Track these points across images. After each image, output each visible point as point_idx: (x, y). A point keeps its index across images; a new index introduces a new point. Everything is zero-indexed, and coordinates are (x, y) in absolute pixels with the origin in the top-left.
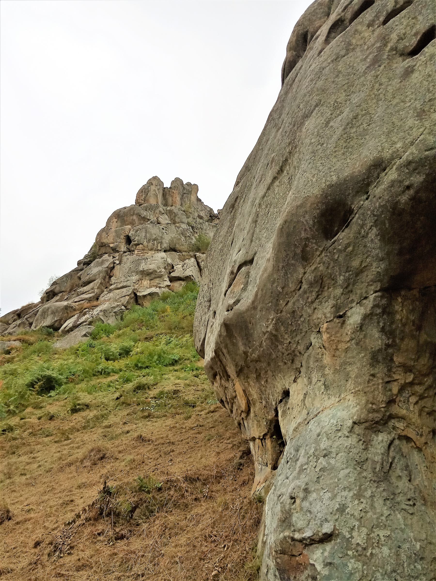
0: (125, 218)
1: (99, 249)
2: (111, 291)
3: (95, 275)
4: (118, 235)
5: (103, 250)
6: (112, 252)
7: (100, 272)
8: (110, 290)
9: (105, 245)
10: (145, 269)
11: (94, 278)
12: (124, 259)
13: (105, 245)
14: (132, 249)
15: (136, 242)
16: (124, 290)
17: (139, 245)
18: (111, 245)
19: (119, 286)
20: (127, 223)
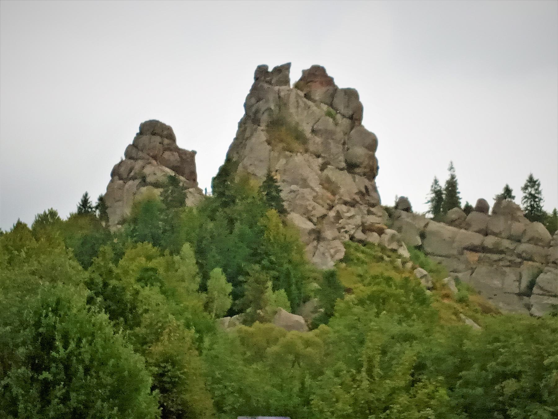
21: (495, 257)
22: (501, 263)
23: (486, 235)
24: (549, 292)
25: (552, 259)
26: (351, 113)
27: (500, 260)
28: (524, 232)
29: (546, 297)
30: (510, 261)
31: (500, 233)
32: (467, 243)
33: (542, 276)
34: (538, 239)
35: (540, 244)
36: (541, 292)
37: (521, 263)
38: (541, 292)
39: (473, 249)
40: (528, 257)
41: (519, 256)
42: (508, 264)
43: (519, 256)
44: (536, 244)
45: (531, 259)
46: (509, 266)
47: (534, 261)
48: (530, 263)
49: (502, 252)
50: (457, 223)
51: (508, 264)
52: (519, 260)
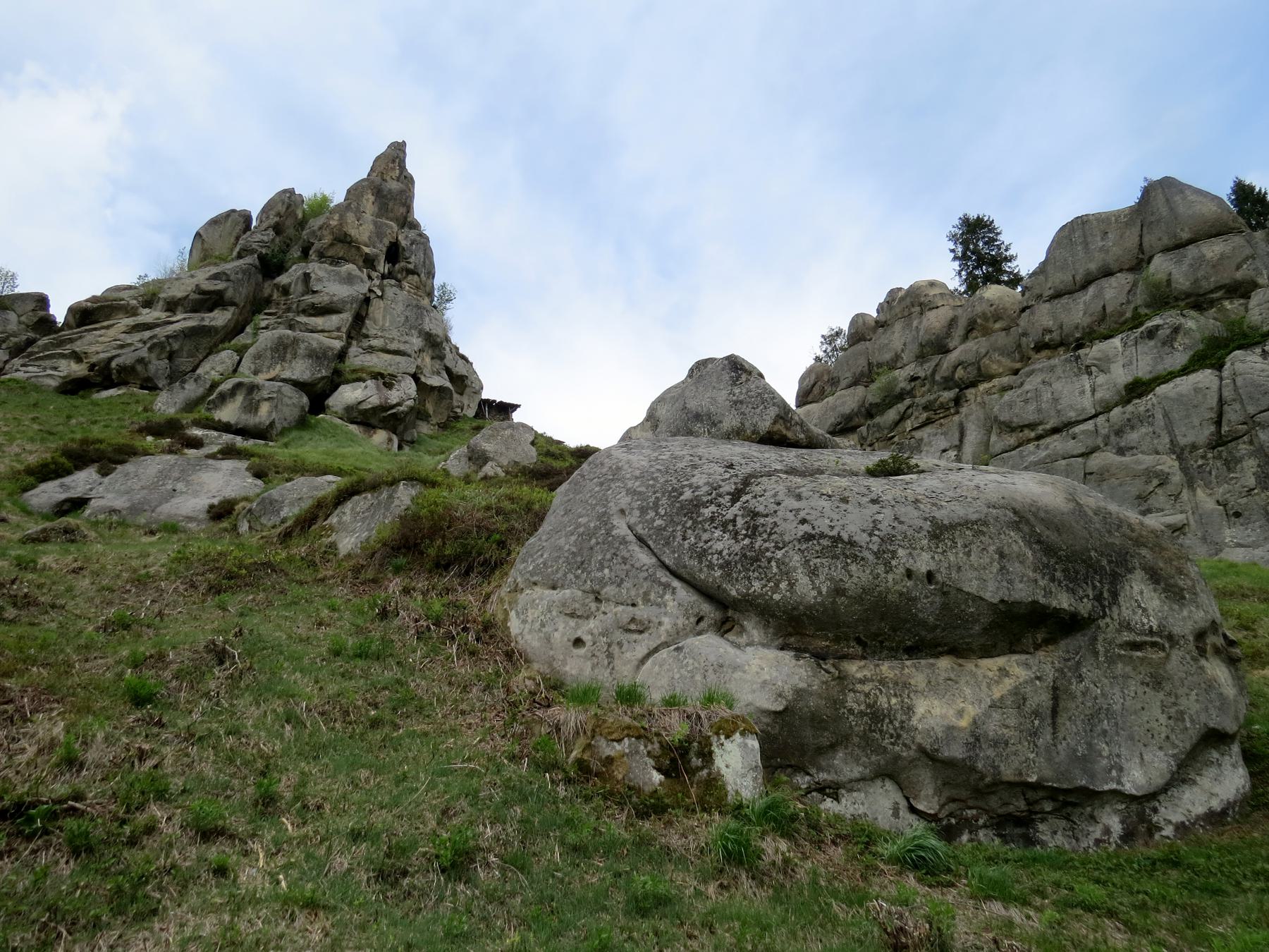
0: (391, 204)
1: (332, 245)
2: (371, 350)
3: (344, 302)
4: (379, 234)
5: (339, 250)
6: (361, 263)
7: (354, 300)
8: (371, 347)
9: (350, 243)
10: (434, 332)
11: (340, 306)
12: (390, 292)
13: (350, 243)
14: (399, 276)
15: (411, 266)
16: (398, 358)
17: (412, 272)
18: (367, 250)
19: (393, 346)
20: (391, 215)
21: (892, 415)
22: (908, 425)
24: (1032, 426)
25: (1029, 342)
27: (903, 417)
29: (1031, 447)
30: (926, 408)
31: (897, 357)
34: (984, 316)
35: (997, 326)
36: (1011, 440)
37: (957, 401)
41: (948, 383)
42: (925, 415)
43: (948, 383)
44: (986, 332)
45: (984, 376)
46: (928, 422)
47: (990, 378)
49: (901, 397)
50: (816, 390)
51: (925, 415)
52: (947, 395)
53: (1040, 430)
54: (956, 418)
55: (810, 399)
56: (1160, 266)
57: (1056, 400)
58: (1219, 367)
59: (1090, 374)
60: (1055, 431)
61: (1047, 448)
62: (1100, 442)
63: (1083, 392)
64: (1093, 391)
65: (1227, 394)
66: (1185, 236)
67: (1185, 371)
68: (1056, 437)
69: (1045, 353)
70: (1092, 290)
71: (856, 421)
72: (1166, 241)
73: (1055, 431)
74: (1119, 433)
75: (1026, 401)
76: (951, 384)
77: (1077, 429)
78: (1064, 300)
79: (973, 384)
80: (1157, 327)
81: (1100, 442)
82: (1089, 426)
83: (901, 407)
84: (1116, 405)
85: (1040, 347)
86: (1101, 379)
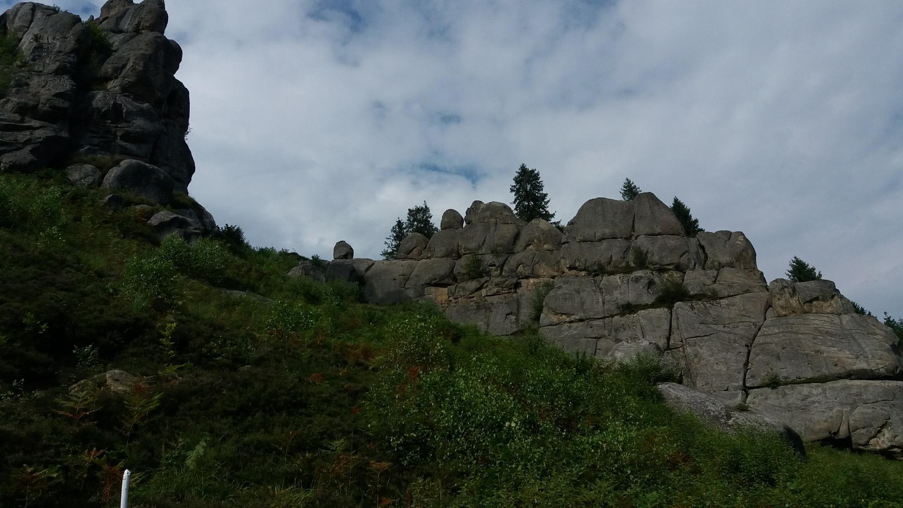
21: (473, 284)
22: (484, 292)
23: (459, 257)
26: (136, 21)
28: (517, 236)
32: (426, 278)
33: (552, 293)
35: (546, 246)
36: (555, 319)
37: (517, 285)
38: (555, 319)
39: (439, 283)
40: (528, 272)
47: (538, 277)
48: (532, 281)
51: (495, 290)
53: (572, 318)
54: (515, 295)
55: (410, 256)
56: (642, 242)
57: (583, 304)
58: (670, 308)
59: (602, 293)
60: (581, 320)
61: (575, 329)
62: (606, 332)
63: (598, 302)
64: (604, 303)
65: (674, 324)
66: (658, 230)
67: (653, 306)
68: (581, 323)
69: (574, 272)
70: (605, 244)
71: (446, 281)
72: (648, 230)
73: (581, 320)
74: (617, 330)
75: (566, 299)
76: (514, 274)
77: (594, 323)
78: (588, 244)
79: (527, 277)
80: (641, 277)
81: (606, 332)
82: (600, 322)
83: (483, 280)
84: (616, 315)
85: (570, 268)
86: (607, 298)
